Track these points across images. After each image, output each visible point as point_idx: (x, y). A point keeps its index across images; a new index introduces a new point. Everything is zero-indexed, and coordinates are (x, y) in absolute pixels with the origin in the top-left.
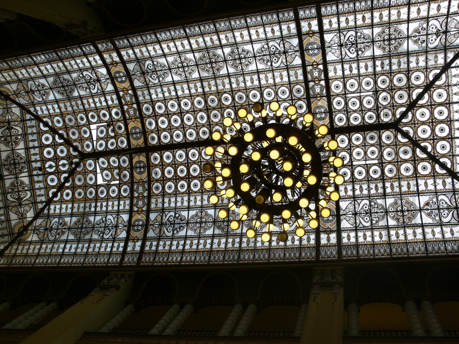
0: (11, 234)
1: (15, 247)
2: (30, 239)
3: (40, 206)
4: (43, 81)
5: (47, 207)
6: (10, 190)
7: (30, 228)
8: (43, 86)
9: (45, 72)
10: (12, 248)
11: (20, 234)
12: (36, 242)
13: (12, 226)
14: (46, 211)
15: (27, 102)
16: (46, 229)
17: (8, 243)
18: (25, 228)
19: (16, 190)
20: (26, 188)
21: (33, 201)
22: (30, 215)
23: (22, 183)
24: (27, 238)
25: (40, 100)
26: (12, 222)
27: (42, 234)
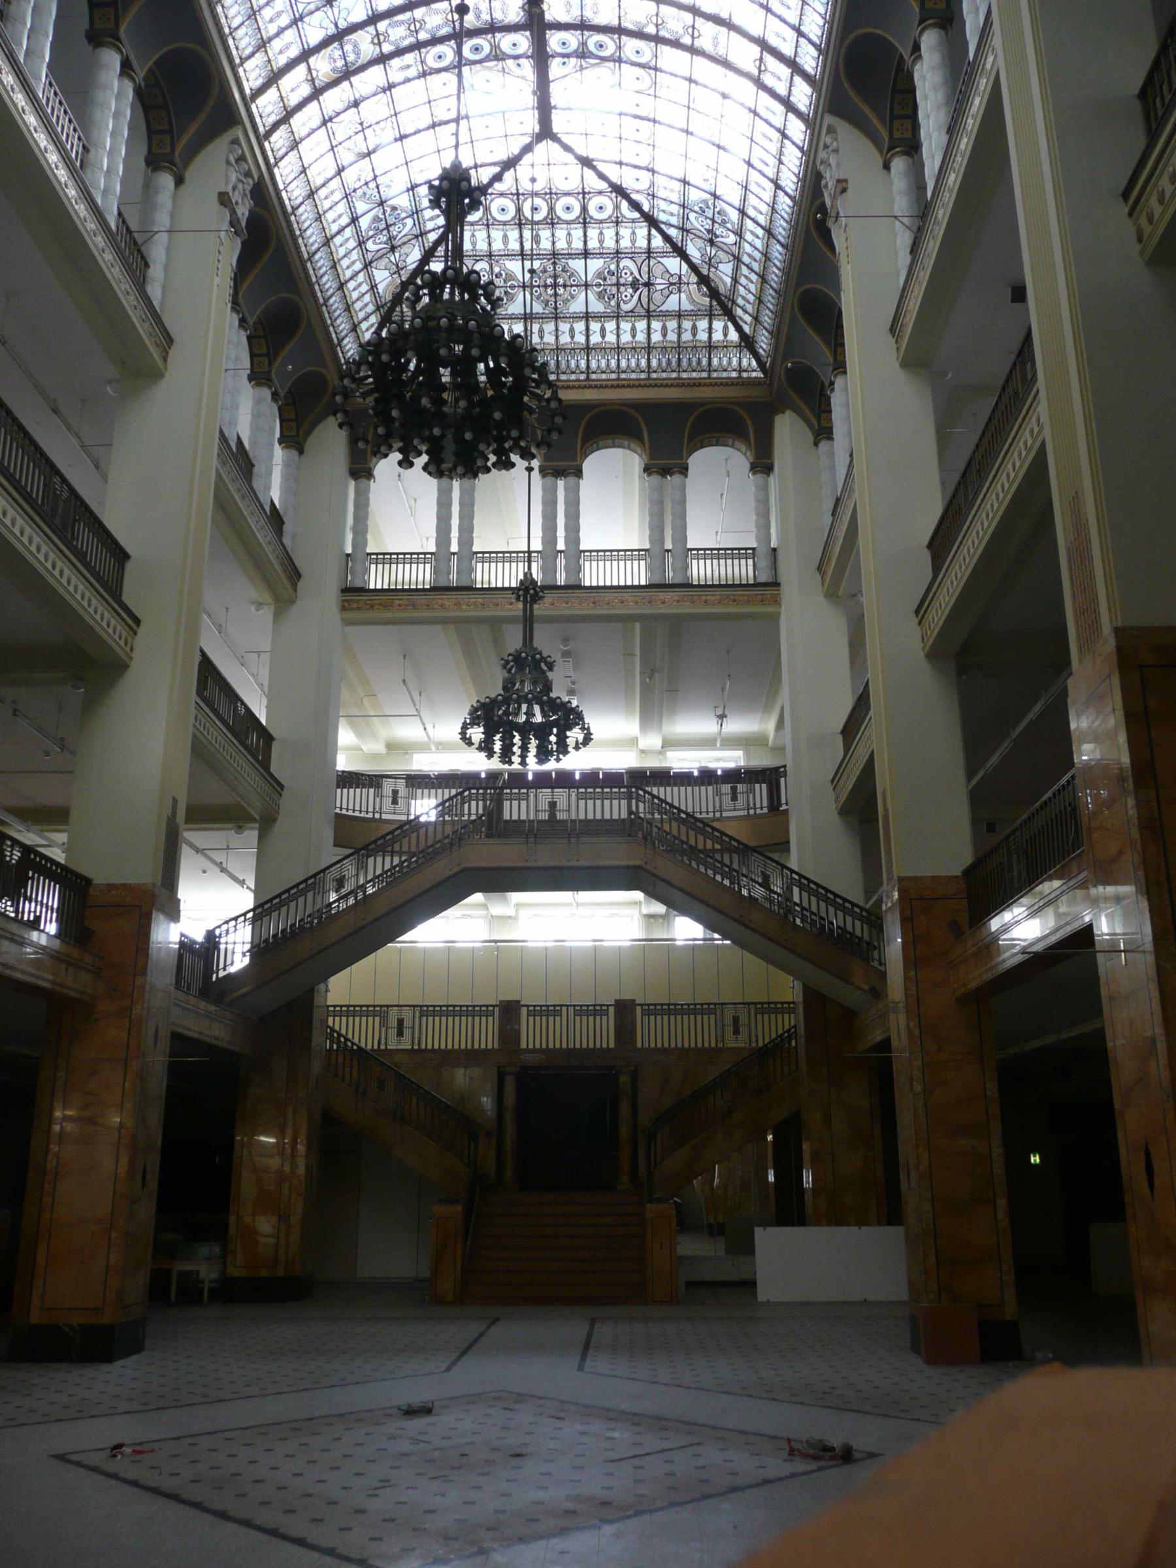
0: (711, 316)
1: (739, 312)
2: (728, 281)
3: (658, 242)
4: (364, 223)
5: (663, 226)
6: (613, 303)
7: (705, 272)
8: (376, 219)
9: (345, 220)
10: (741, 318)
11: (714, 293)
12: (736, 269)
13: (692, 308)
14: (673, 232)
15: (417, 248)
16: (711, 242)
17: (729, 324)
18: (704, 280)
19: (614, 290)
20: (613, 267)
21: (644, 256)
22: (674, 264)
23: (599, 274)
24: (725, 284)
25: (409, 222)
26: (683, 308)
27: (720, 253)
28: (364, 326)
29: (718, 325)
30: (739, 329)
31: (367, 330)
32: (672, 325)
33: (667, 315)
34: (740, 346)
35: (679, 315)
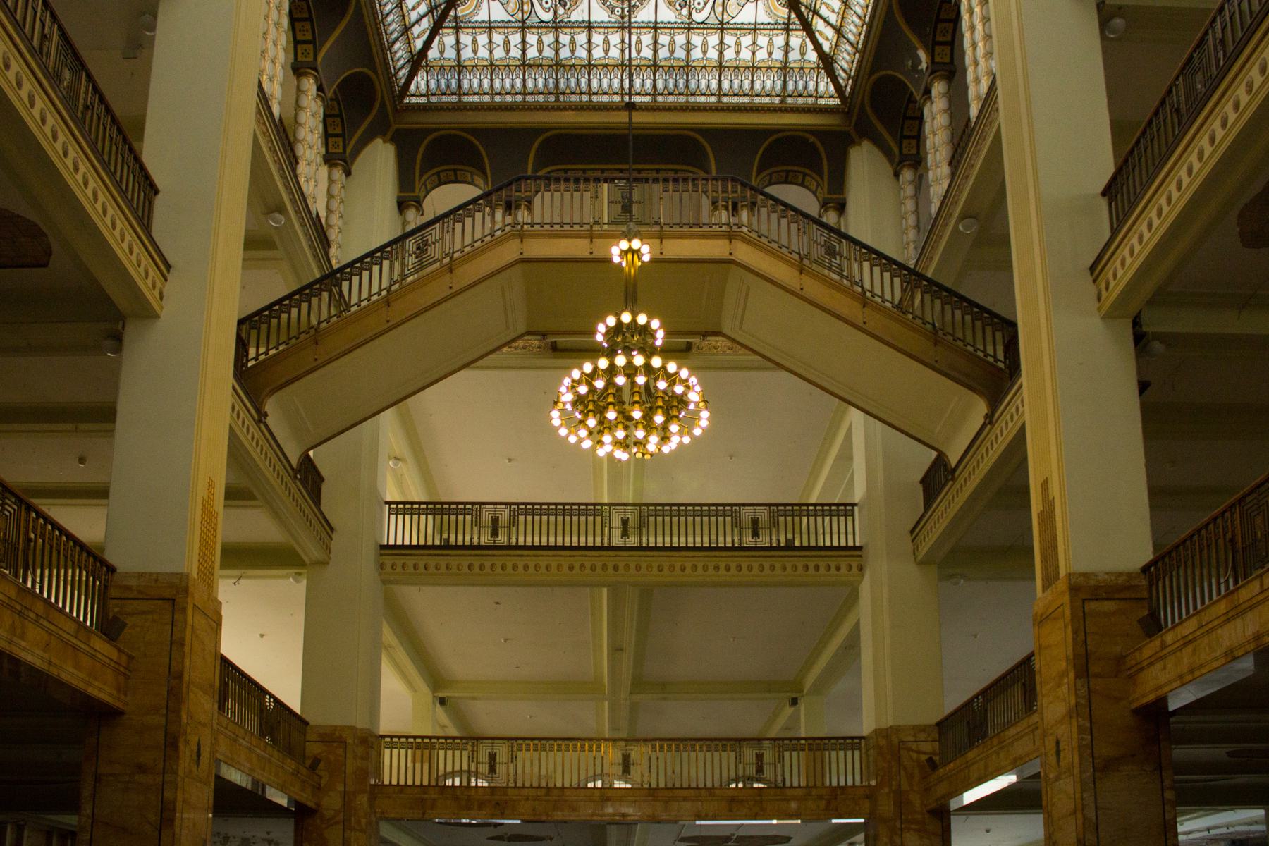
0: (787, 29)
1: (819, 25)
6: (685, 11)
13: (770, 20)
17: (808, 40)
26: (759, 21)
28: (416, 30)
29: (795, 41)
30: (818, 47)
31: (419, 37)
32: (747, 40)
33: (740, 29)
34: (818, 67)
35: (755, 29)
